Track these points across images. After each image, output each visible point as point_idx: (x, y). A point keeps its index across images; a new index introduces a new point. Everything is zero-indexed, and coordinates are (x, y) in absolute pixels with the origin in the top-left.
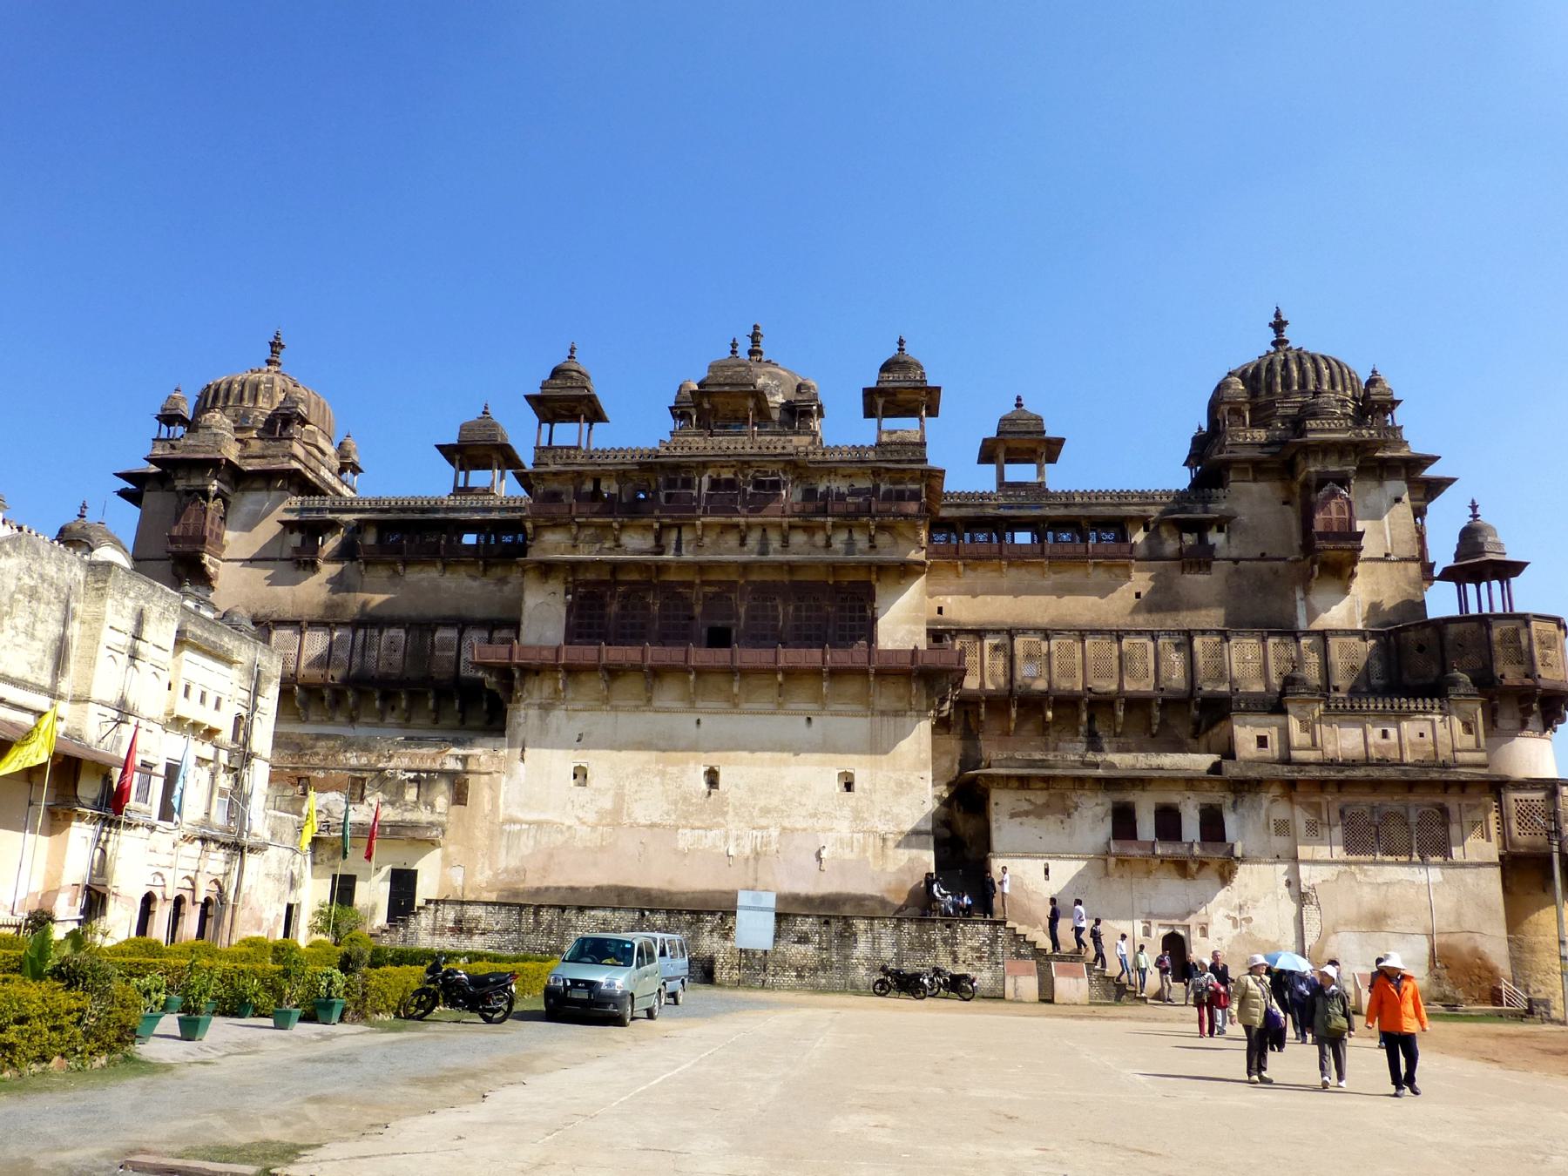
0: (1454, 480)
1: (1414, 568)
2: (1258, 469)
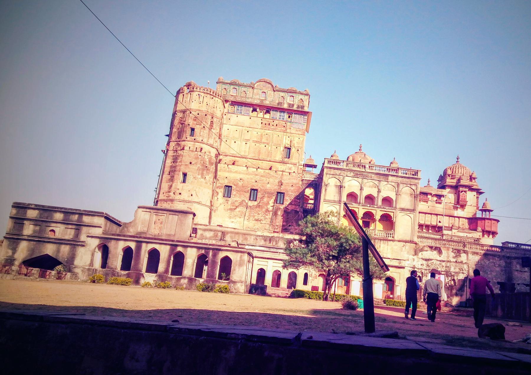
0: (484, 193)
1: (476, 208)
2: (451, 187)
